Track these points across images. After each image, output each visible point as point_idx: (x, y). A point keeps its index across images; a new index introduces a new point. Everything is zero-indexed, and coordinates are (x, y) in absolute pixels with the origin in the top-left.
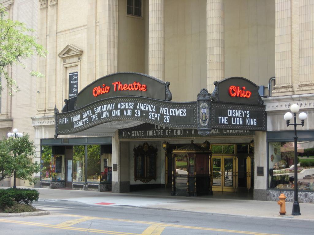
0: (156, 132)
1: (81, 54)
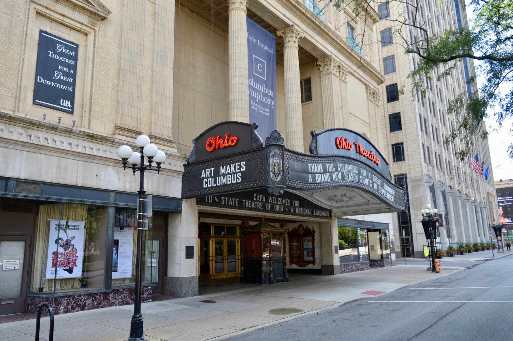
0: (255, 203)
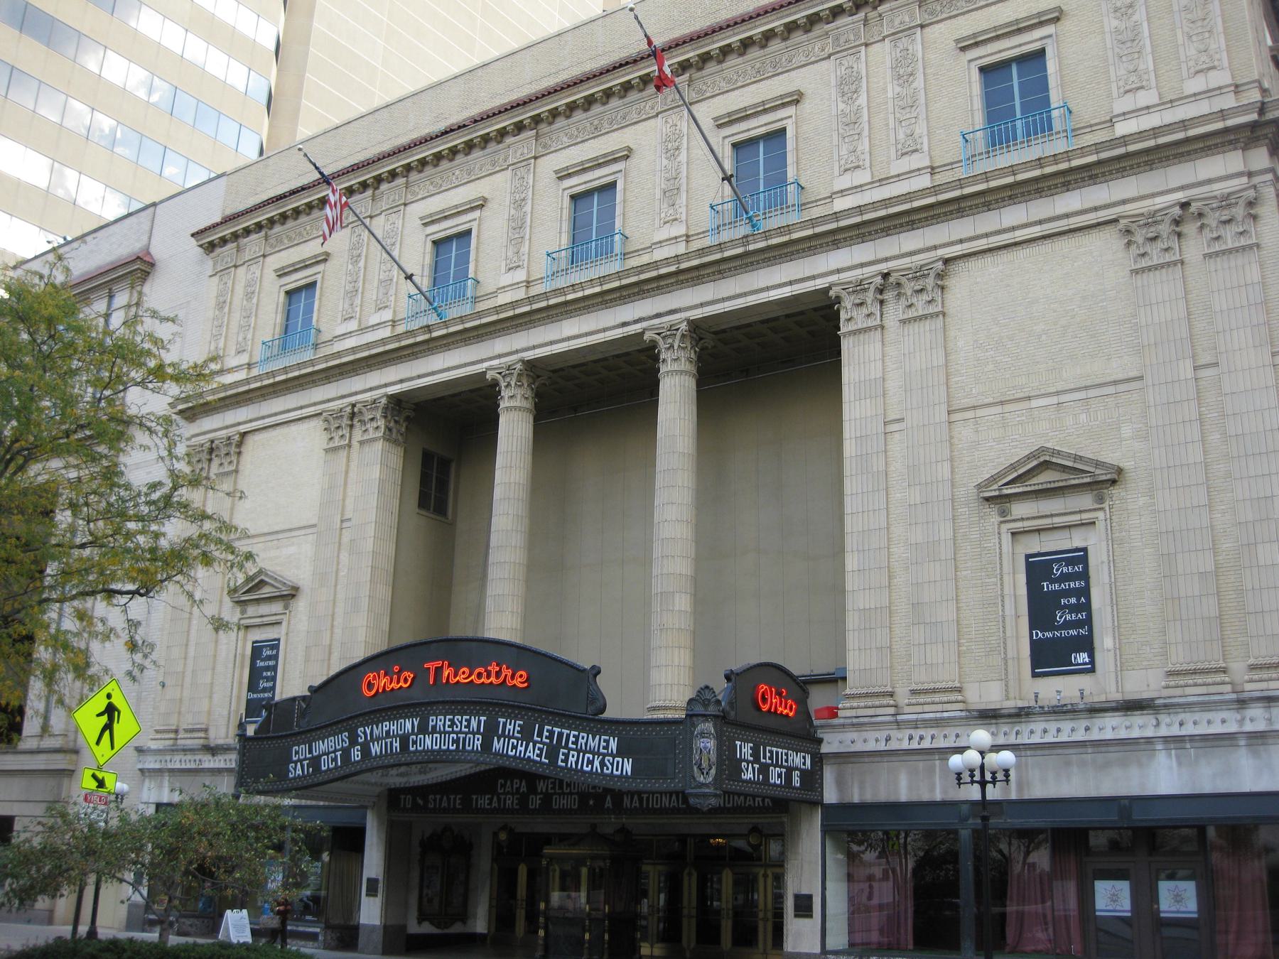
0: (499, 800)
1: (293, 596)
